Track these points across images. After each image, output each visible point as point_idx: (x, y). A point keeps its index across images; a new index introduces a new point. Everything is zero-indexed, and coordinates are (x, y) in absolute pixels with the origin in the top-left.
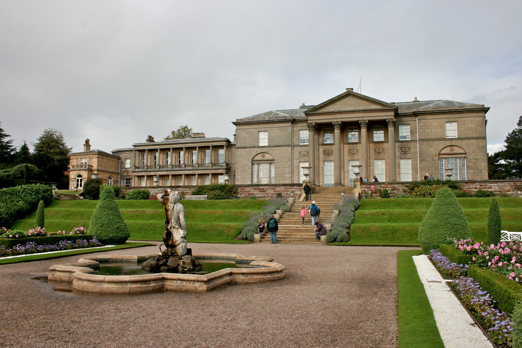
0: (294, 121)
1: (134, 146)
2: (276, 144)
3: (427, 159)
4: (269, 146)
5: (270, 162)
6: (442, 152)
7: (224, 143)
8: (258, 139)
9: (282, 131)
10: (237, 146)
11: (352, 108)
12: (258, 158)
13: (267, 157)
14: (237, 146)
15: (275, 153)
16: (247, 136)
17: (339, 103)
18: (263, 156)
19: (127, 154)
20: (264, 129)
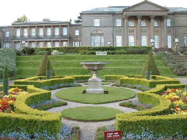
0: (113, 14)
1: (12, 24)
2: (104, 25)
3: (179, 36)
4: (100, 27)
5: (101, 35)
6: (185, 32)
7: (68, 24)
8: (94, 23)
9: (108, 19)
10: (82, 26)
11: (147, 9)
12: (94, 32)
13: (99, 32)
14: (82, 26)
15: (104, 30)
16: (88, 21)
17: (140, 6)
18: (97, 32)
19: (7, 29)
20: (97, 18)
